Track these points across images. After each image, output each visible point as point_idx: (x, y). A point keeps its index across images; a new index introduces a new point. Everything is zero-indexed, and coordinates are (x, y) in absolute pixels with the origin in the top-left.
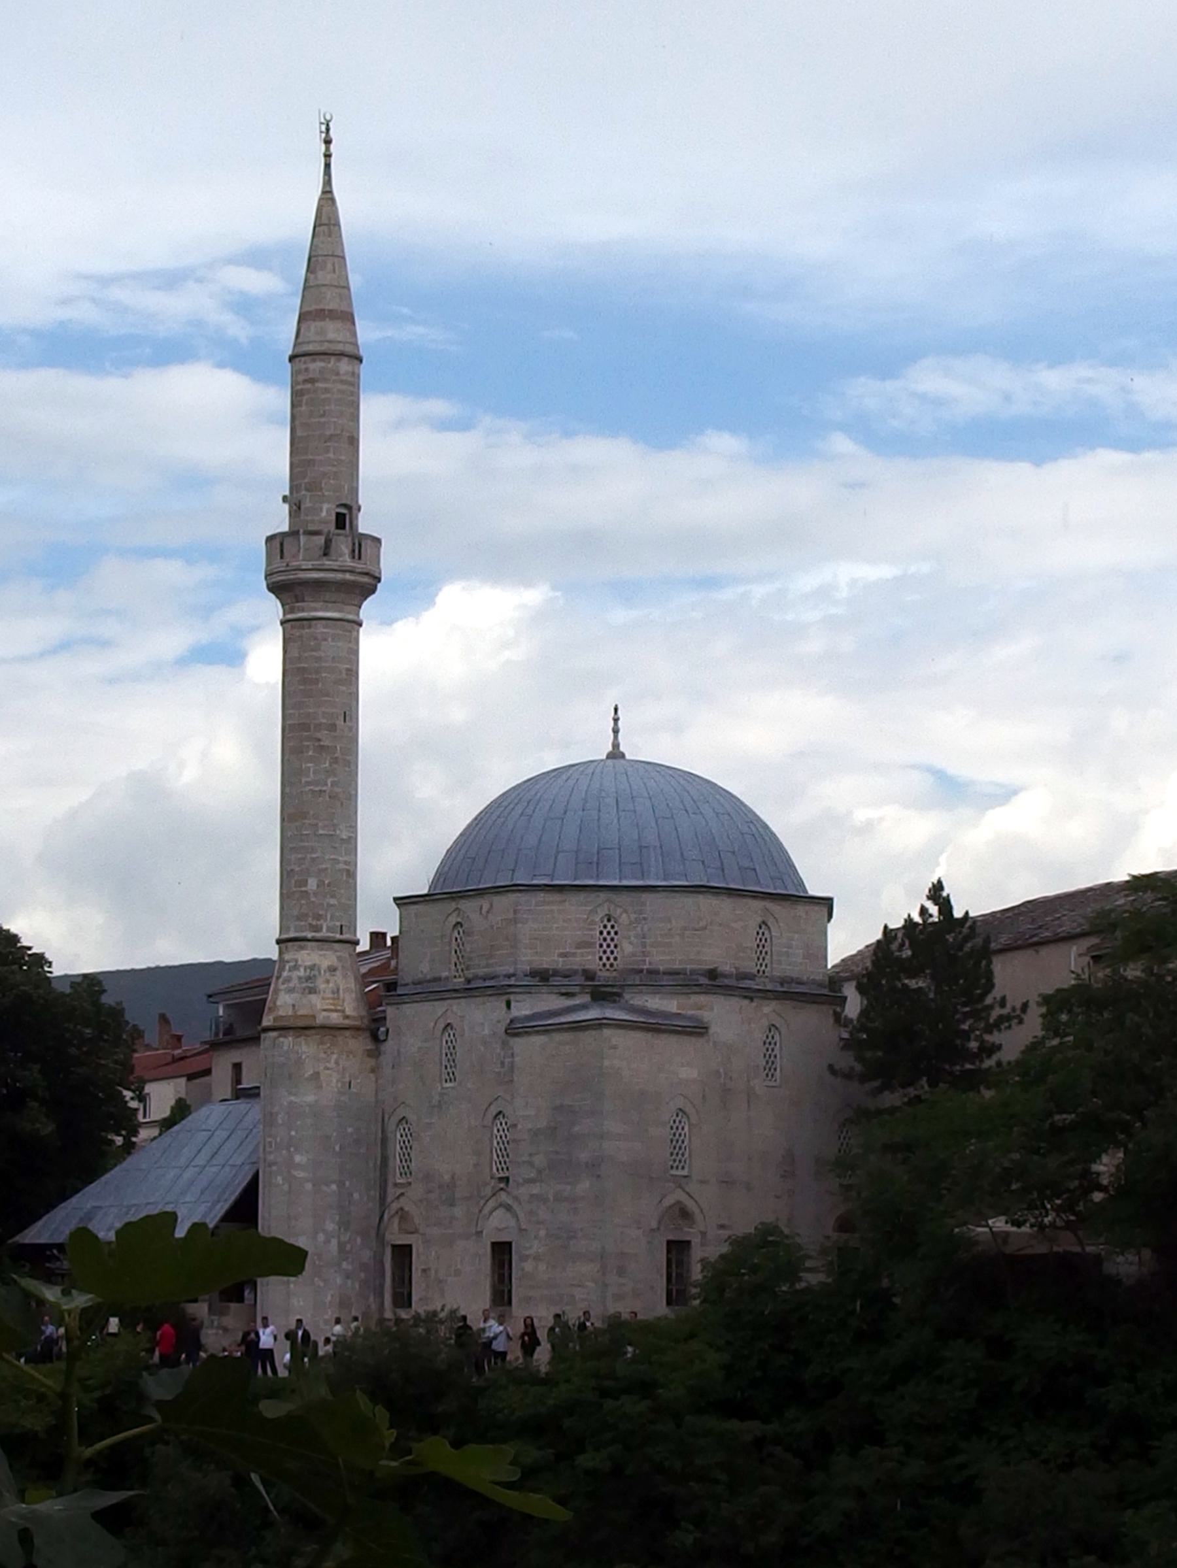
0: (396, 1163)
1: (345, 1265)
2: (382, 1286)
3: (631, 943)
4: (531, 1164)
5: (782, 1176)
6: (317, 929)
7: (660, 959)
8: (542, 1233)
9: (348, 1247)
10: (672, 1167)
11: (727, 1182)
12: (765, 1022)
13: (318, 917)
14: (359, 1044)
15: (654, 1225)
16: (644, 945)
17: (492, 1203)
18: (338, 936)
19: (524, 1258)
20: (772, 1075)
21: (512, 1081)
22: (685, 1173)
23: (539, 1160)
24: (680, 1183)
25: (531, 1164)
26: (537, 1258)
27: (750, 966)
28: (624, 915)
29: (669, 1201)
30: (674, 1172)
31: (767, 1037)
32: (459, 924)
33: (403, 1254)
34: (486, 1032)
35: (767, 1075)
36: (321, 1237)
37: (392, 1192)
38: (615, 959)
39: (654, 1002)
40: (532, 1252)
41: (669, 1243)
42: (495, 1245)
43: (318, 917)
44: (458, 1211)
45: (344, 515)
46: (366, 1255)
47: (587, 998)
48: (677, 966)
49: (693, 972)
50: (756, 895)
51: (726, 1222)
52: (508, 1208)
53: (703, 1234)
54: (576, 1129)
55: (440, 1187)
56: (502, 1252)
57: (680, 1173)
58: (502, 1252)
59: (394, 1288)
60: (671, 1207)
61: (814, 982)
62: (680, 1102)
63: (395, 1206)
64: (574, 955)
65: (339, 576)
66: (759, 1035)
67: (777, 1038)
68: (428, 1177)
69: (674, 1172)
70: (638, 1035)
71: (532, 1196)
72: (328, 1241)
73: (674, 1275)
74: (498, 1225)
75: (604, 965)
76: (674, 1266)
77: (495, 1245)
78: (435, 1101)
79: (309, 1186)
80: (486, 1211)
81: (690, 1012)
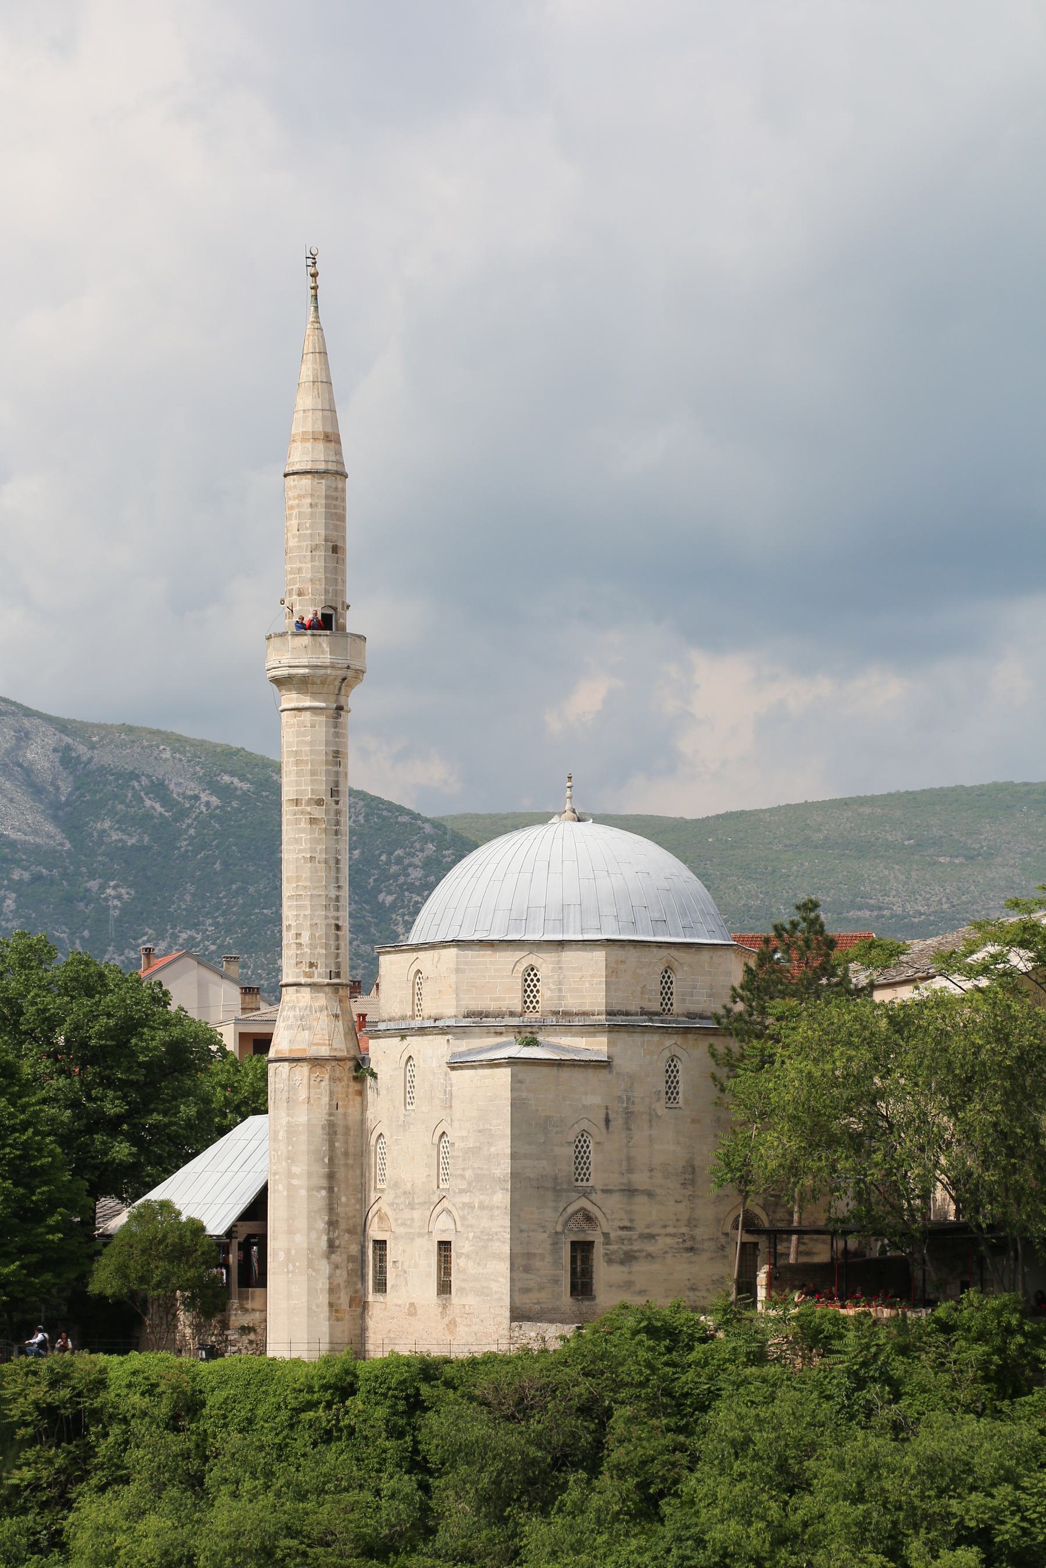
3: (549, 989)
4: (463, 1177)
5: (683, 1184)
7: (572, 1003)
8: (471, 1235)
9: (337, 1243)
10: (577, 1180)
11: (630, 1192)
12: (667, 1054)
15: (559, 1229)
16: (560, 990)
17: (439, 1208)
18: (327, 981)
19: (459, 1256)
20: (675, 1099)
21: (451, 1107)
22: (590, 1184)
24: (585, 1193)
25: (463, 1177)
26: (468, 1256)
27: (656, 1007)
28: (544, 965)
29: (571, 1210)
30: (579, 1183)
31: (670, 1066)
32: (419, 971)
33: (381, 1245)
34: (434, 1065)
35: (669, 1099)
36: (314, 1235)
38: (537, 1002)
39: (567, 1041)
40: (464, 1251)
41: (573, 1243)
42: (440, 1243)
44: (417, 1214)
45: (331, 615)
50: (660, 945)
51: (627, 1224)
52: (449, 1212)
53: (606, 1235)
55: (405, 1193)
56: (444, 1246)
57: (584, 1183)
58: (444, 1246)
59: (375, 1277)
60: (576, 1212)
62: (585, 1125)
64: (504, 999)
65: (322, 672)
66: (662, 1066)
67: (680, 1066)
68: (396, 1185)
69: (579, 1183)
70: (545, 1070)
71: (464, 1203)
73: (579, 1269)
74: (443, 1228)
75: (528, 1007)
76: (579, 1263)
79: (303, 1192)
81: (596, 1048)
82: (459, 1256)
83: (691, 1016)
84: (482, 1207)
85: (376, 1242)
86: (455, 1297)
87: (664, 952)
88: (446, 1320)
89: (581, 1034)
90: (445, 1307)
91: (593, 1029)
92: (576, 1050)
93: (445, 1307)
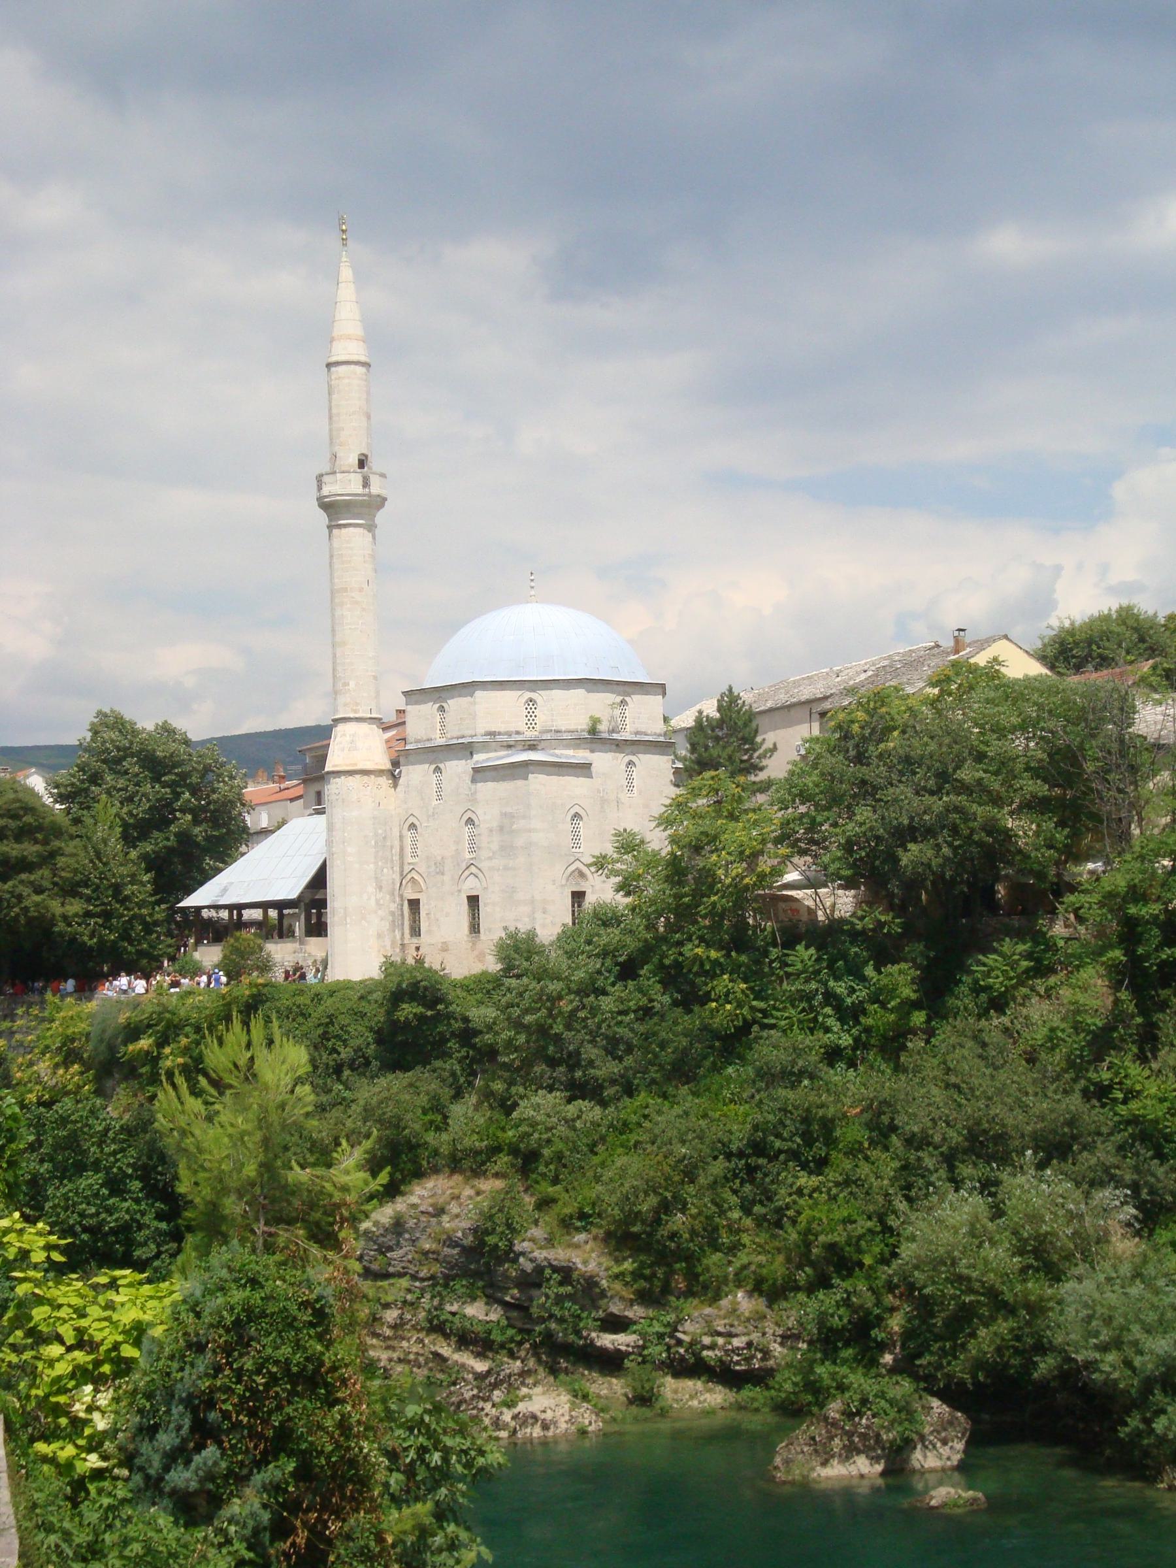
0: (408, 850)
1: (380, 912)
2: (403, 924)
6: (356, 711)
7: (563, 724)
13: (357, 704)
14: (385, 781)
15: (564, 882)
17: (467, 873)
23: (495, 846)
33: (414, 904)
37: (407, 868)
42: (469, 897)
43: (357, 704)
44: (446, 878)
46: (393, 907)
47: (521, 747)
48: (572, 727)
49: (583, 731)
54: (514, 827)
56: (473, 901)
58: (473, 901)
61: (655, 734)
63: (409, 876)
72: (369, 899)
74: (471, 886)
77: (469, 897)
78: (430, 813)
80: (463, 877)
82: (486, 905)
83: (637, 733)
84: (506, 868)
85: (410, 901)
86: (483, 936)
87: (621, 688)
88: (476, 953)
89: (567, 747)
90: (474, 944)
91: (578, 742)
92: (567, 757)
93: (474, 944)
